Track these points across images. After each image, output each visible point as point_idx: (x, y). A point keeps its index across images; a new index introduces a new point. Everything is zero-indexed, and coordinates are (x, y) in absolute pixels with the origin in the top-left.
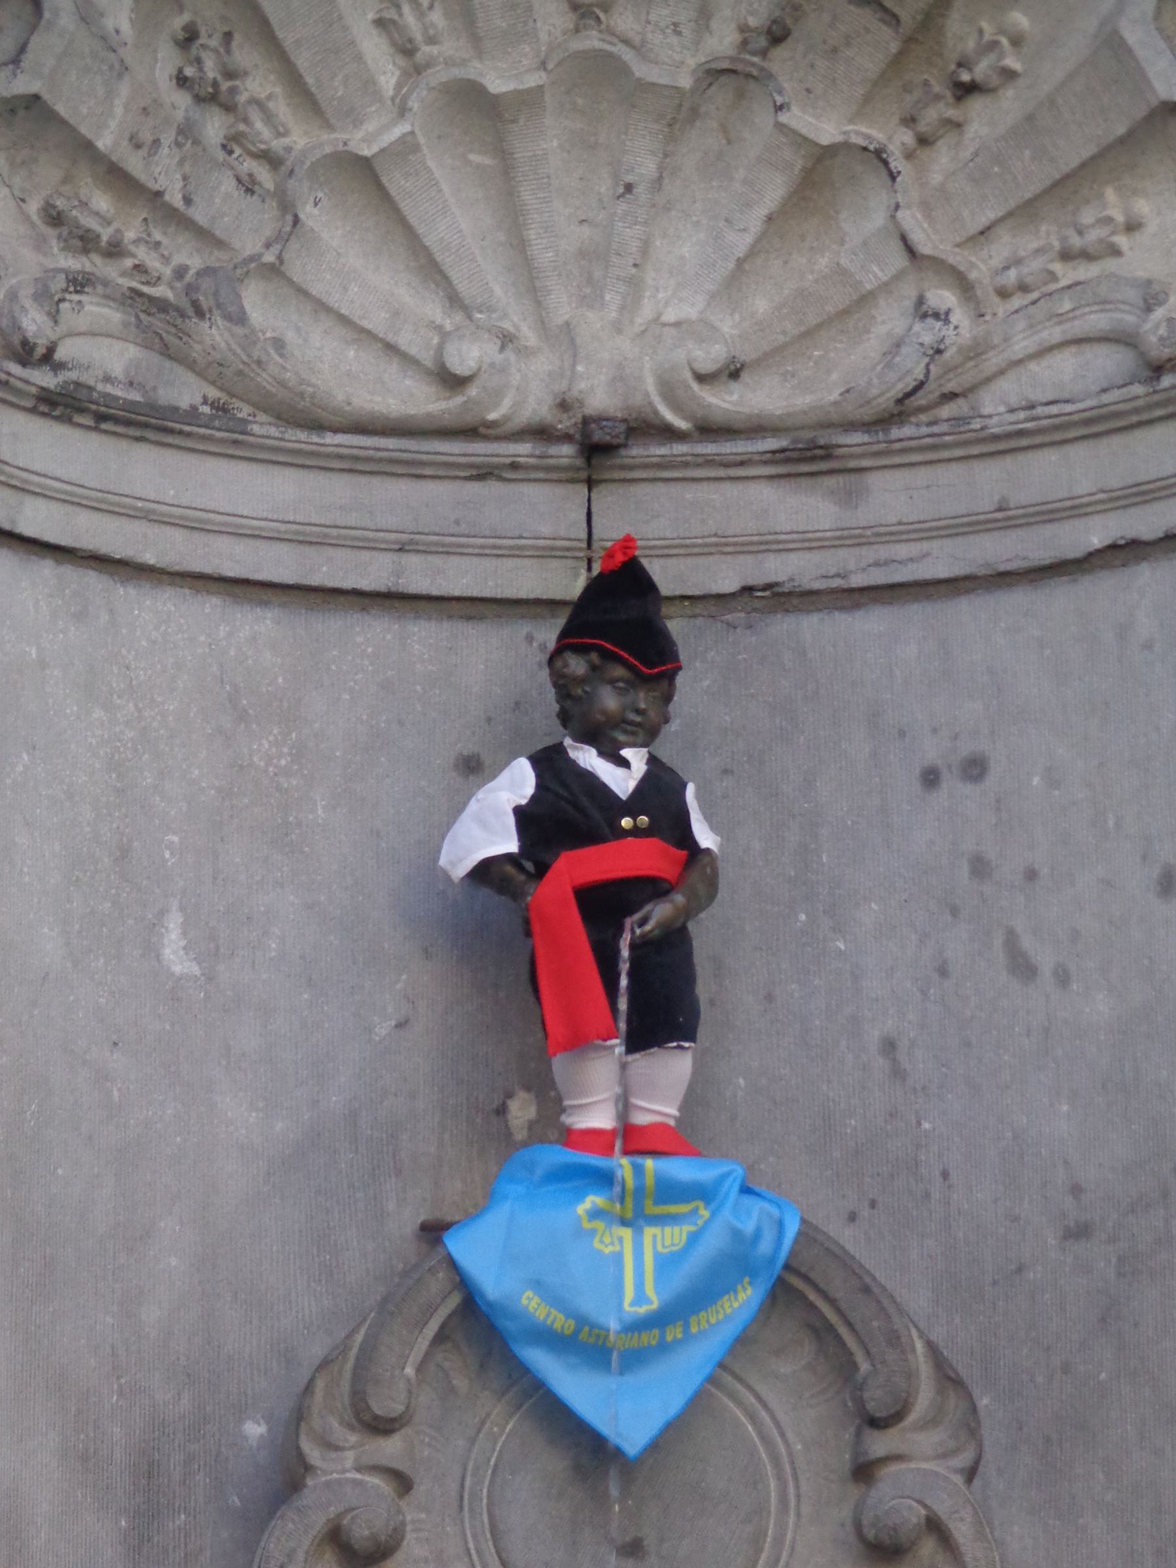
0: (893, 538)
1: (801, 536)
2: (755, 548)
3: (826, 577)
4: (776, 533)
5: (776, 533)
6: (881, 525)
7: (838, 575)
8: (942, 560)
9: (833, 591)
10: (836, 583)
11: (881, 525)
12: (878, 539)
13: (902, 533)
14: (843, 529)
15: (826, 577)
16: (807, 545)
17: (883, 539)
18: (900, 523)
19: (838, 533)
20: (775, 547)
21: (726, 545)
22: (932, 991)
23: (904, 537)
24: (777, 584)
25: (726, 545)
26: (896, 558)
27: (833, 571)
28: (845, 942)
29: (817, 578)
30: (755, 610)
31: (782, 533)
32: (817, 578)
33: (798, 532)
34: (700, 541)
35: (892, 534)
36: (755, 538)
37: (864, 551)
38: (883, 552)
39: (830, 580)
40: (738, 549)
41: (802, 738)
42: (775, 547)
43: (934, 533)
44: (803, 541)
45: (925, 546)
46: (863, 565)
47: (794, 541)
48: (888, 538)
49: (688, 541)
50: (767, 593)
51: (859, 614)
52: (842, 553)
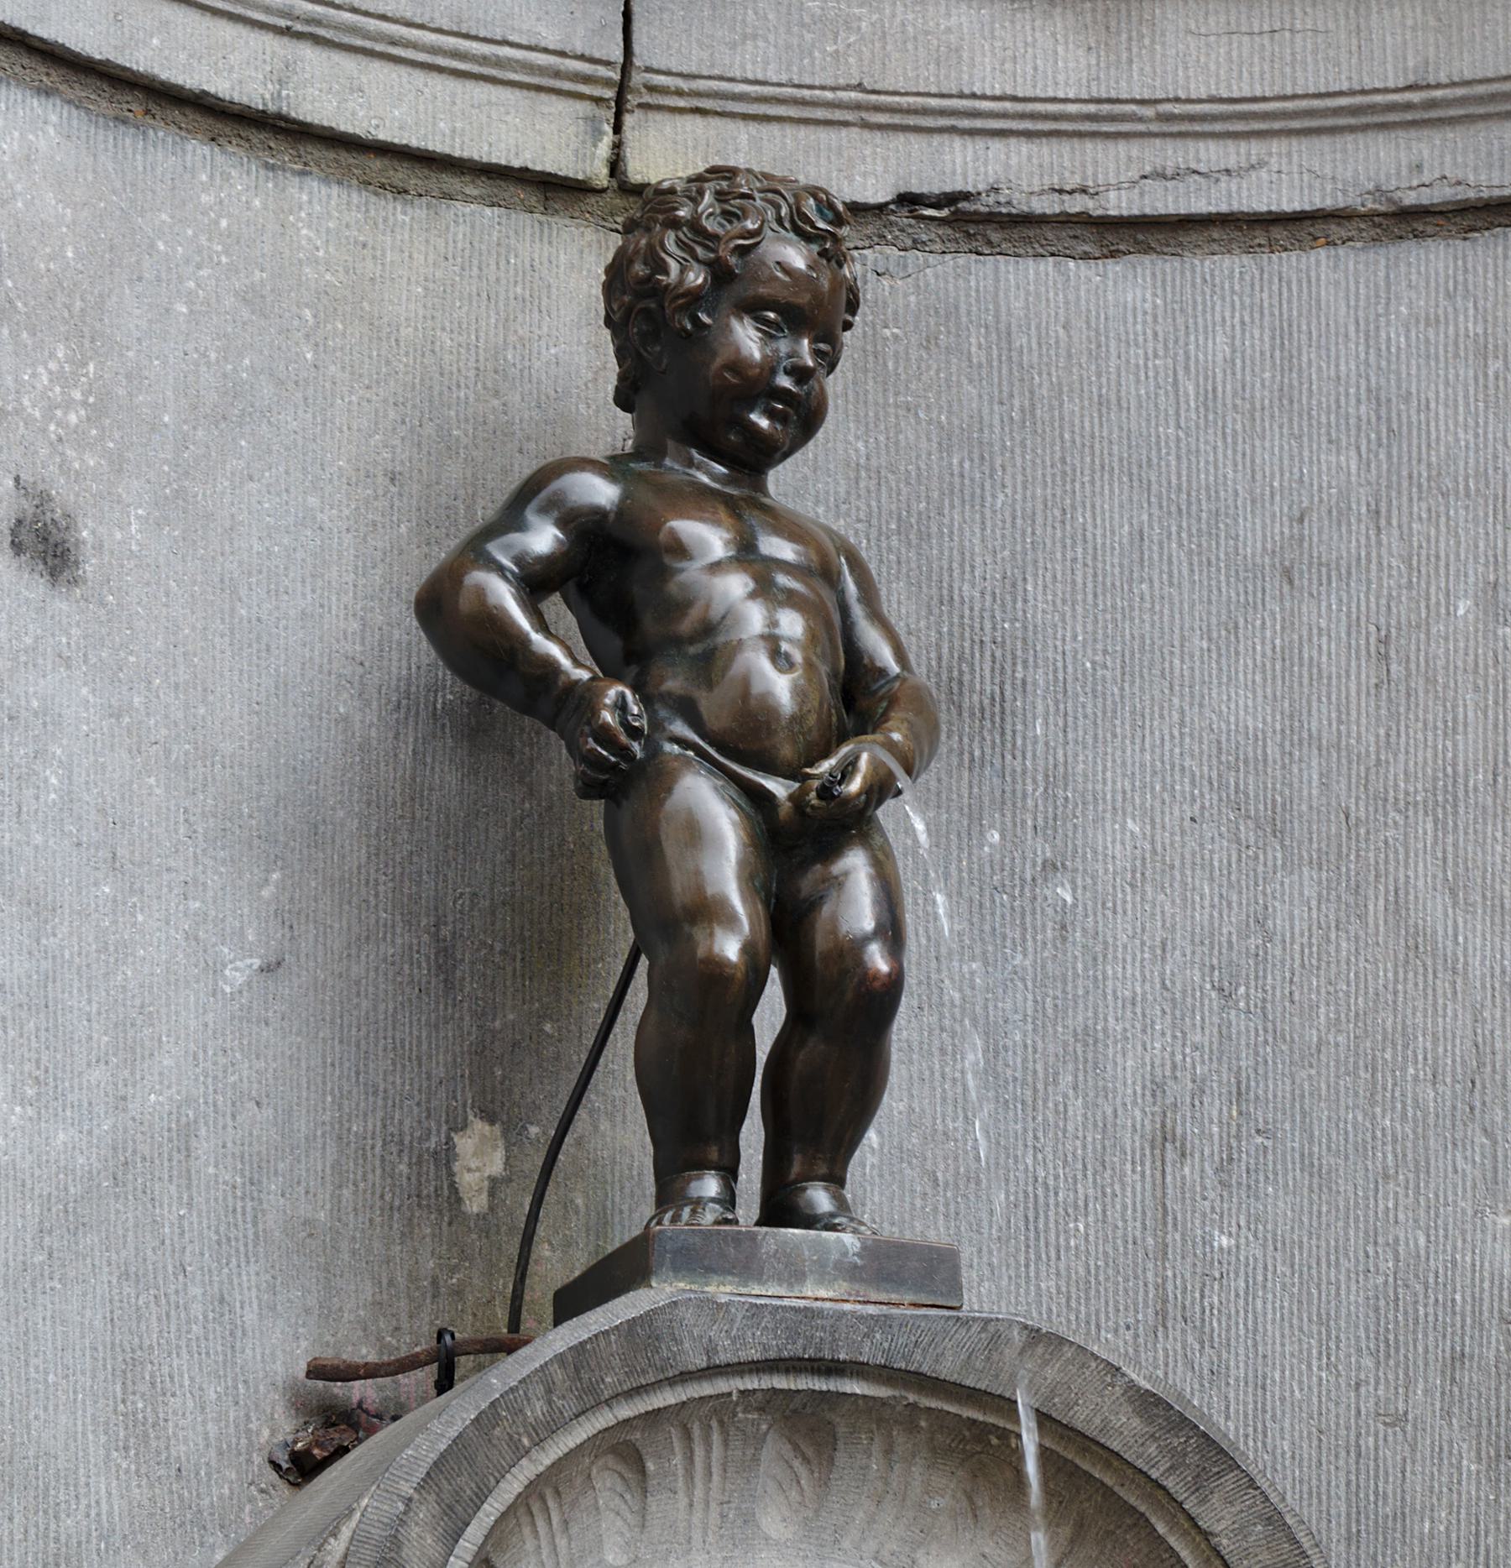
0: (1197, 127)
1: (1019, 107)
2: (928, 122)
3: (1061, 191)
4: (974, 96)
5: (974, 96)
6: (1177, 100)
7: (1084, 191)
8: (1282, 179)
9: (1065, 220)
10: (1076, 205)
11: (1177, 100)
12: (1166, 128)
13: (1214, 118)
14: (1099, 101)
15: (1061, 191)
16: (1028, 125)
17: (1175, 128)
18: (1212, 100)
19: (1092, 108)
20: (966, 123)
21: (877, 108)
22: (1242, 990)
23: (1218, 127)
24: (966, 196)
25: (877, 108)
26: (1193, 166)
27: (1073, 182)
28: (1074, 890)
29: (1042, 193)
30: (917, 245)
31: (984, 97)
32: (1042, 193)
33: (1015, 99)
34: (829, 95)
35: (1192, 118)
36: (934, 102)
37: (1135, 148)
38: (1173, 154)
39: (1066, 197)
40: (897, 119)
41: (1001, 497)
42: (966, 123)
43: (1277, 125)
44: (1022, 116)
45: (1256, 148)
46: (1134, 174)
47: (1004, 115)
48: (1185, 127)
49: (806, 93)
50: (945, 213)
51: (1114, 267)
52: (1089, 145)
